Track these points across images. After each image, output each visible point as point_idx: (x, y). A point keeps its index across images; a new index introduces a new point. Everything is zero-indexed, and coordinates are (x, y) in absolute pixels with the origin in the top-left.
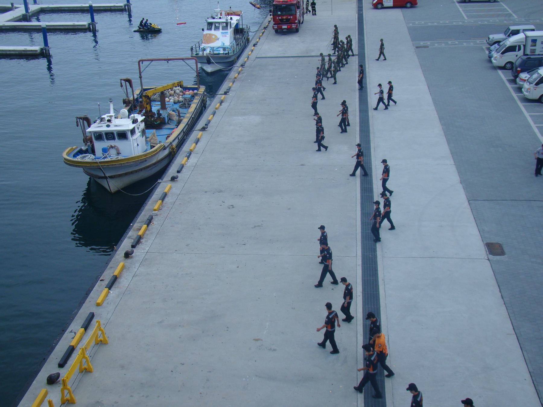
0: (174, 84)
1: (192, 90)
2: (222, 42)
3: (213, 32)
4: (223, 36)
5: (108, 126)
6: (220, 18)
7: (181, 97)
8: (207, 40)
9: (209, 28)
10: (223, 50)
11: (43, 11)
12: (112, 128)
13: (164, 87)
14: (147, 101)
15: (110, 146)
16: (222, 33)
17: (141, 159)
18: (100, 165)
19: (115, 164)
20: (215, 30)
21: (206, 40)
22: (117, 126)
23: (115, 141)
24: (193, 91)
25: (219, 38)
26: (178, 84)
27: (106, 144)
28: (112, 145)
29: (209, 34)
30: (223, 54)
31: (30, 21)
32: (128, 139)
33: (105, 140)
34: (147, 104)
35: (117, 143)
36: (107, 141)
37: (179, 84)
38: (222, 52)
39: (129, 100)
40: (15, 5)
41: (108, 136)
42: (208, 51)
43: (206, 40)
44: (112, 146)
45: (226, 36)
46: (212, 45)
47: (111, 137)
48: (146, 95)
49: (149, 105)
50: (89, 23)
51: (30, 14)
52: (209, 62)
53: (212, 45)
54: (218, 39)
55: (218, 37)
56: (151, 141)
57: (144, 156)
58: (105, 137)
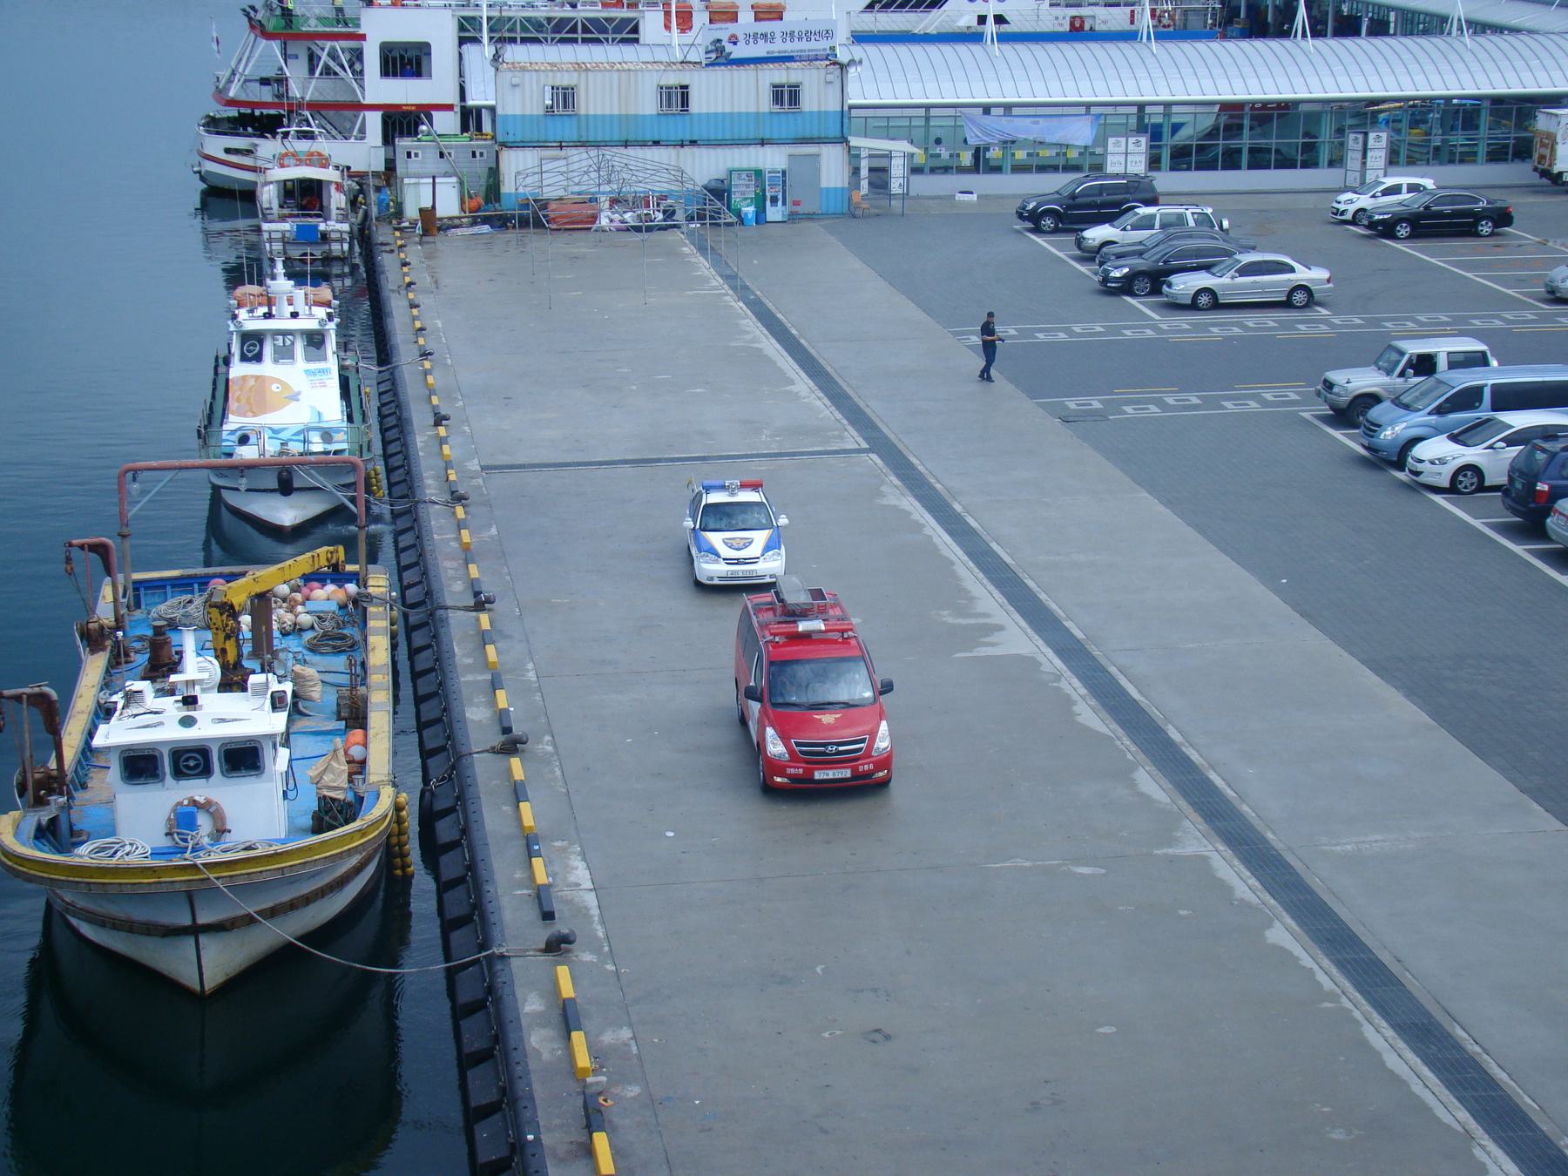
0: (316, 558)
1: (332, 583)
5: (187, 722)
7: (300, 608)
13: (283, 568)
14: (227, 625)
15: (186, 802)
17: (349, 850)
18: (211, 876)
19: (261, 872)
22: (223, 720)
24: (340, 587)
26: (329, 555)
27: (169, 795)
28: (197, 798)
32: (263, 772)
33: (169, 779)
35: (218, 789)
36: (175, 782)
37: (332, 558)
41: (181, 764)
44: (195, 801)
47: (196, 766)
48: (225, 600)
49: (233, 639)
56: (321, 777)
57: (360, 834)
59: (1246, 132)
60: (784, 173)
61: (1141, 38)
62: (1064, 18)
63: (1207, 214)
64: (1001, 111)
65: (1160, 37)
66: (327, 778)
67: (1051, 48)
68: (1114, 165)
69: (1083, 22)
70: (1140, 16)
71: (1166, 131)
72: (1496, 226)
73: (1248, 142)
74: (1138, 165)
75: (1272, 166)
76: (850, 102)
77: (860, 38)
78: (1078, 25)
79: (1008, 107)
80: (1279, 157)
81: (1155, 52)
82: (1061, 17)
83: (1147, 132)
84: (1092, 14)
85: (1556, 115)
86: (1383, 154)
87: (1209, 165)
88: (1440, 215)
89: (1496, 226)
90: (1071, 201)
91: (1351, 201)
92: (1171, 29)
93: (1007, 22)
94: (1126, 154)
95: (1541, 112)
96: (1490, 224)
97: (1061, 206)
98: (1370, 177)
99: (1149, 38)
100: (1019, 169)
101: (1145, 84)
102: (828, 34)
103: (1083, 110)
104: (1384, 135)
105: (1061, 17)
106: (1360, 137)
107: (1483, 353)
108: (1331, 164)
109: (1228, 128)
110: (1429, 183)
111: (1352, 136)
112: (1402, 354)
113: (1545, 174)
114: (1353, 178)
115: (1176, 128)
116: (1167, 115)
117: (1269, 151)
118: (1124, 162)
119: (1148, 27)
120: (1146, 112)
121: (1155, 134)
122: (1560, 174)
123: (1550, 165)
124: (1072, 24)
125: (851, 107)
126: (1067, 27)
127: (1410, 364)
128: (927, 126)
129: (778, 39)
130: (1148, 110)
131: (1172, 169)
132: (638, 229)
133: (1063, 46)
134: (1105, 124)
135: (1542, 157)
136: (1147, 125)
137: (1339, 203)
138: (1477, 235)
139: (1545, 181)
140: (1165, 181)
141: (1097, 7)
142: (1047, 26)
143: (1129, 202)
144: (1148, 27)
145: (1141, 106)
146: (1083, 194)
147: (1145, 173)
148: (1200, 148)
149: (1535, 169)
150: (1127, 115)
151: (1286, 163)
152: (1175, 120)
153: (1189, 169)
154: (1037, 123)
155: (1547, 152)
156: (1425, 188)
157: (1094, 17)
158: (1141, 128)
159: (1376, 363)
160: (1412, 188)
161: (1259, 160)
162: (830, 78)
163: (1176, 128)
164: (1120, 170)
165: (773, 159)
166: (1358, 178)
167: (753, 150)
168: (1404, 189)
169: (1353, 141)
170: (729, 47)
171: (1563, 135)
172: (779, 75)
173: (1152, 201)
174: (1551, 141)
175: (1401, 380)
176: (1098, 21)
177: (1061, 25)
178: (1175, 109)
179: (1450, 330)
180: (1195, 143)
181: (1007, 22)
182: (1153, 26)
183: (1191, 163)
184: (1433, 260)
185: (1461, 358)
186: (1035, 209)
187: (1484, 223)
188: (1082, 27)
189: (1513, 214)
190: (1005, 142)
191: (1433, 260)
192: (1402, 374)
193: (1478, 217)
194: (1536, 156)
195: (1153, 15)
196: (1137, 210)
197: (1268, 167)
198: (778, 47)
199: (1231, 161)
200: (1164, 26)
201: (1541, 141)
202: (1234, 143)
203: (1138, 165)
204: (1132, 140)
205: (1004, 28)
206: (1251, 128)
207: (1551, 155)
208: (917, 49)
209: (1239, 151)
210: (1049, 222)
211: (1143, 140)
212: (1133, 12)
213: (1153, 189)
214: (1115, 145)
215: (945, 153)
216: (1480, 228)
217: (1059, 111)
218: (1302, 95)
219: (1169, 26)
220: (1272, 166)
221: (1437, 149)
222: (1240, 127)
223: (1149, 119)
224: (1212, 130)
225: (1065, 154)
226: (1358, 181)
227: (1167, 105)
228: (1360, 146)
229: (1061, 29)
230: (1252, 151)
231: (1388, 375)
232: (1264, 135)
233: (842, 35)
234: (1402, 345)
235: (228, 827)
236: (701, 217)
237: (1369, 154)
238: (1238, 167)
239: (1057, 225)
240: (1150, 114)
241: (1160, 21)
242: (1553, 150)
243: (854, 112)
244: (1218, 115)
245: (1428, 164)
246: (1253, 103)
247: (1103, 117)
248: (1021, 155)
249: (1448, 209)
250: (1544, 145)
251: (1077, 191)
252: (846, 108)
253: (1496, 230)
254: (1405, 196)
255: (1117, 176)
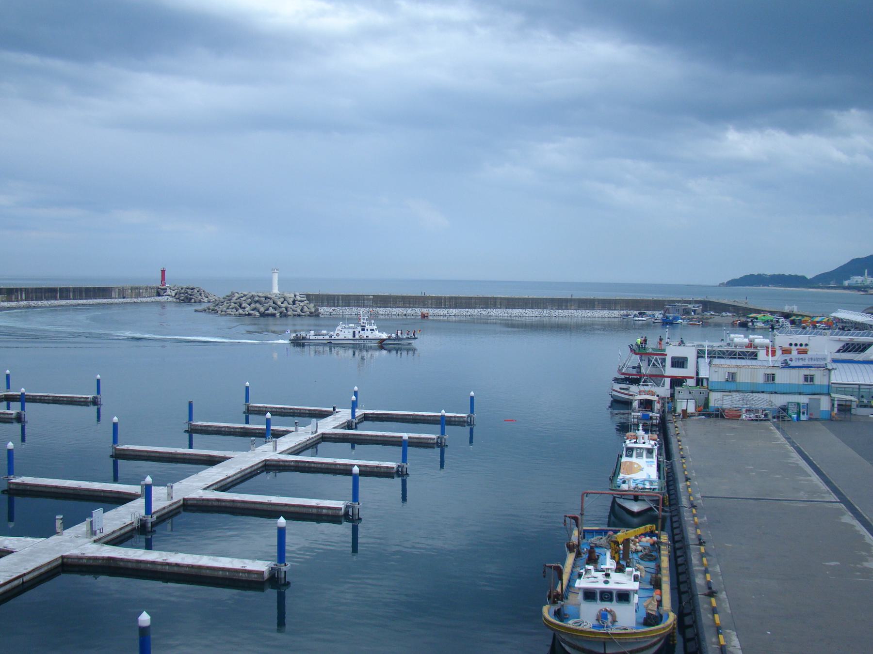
2: (647, 474)
3: (634, 459)
4: (648, 466)
5: (606, 582)
6: (644, 443)
8: (627, 470)
9: (628, 455)
10: (650, 483)
11: (366, 418)
12: (611, 586)
15: (603, 610)
16: (647, 462)
20: (637, 457)
21: (625, 469)
23: (613, 603)
25: (643, 468)
28: (607, 609)
29: (630, 462)
30: (650, 489)
31: (356, 428)
34: (616, 553)
35: (614, 606)
38: (648, 486)
39: (574, 544)
40: (337, 410)
41: (603, 596)
42: (633, 485)
43: (625, 469)
45: (651, 466)
46: (633, 476)
50: (438, 435)
51: (357, 421)
52: (636, 499)
53: (633, 476)
54: (642, 469)
55: (642, 467)
58: (598, 598)
60: (807, 404)
66: (650, 607)
76: (832, 382)
77: (835, 361)
102: (824, 359)
125: (833, 383)
128: (859, 391)
129: (807, 361)
132: (757, 420)
162: (825, 373)
165: (803, 399)
167: (797, 396)
170: (789, 362)
172: (807, 372)
198: (806, 363)
208: (856, 365)
215: (865, 401)
233: (829, 360)
235: (617, 620)
236: (778, 417)
243: (833, 385)
252: (830, 384)
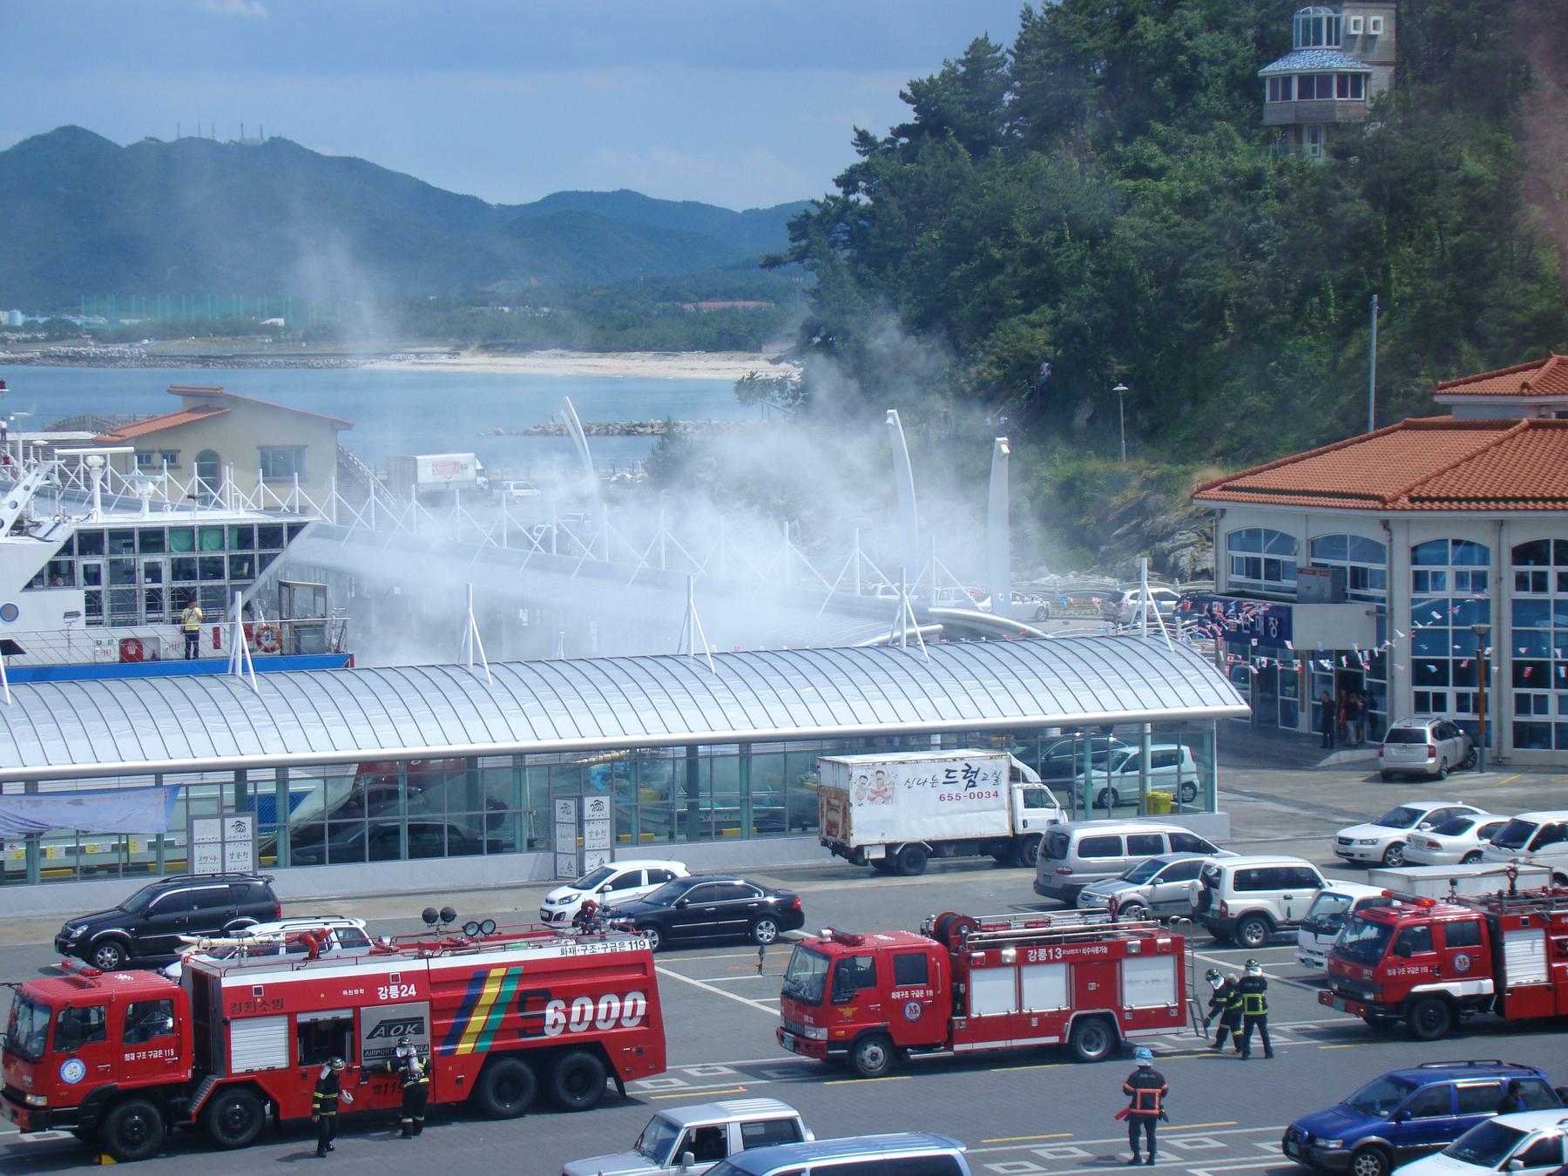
59: (402, 801)
61: (234, 670)
62: (110, 642)
63: (357, 929)
64: (20, 788)
65: (262, 666)
67: (92, 687)
68: (206, 862)
69: (140, 647)
70: (228, 636)
71: (281, 804)
72: (782, 927)
73: (407, 817)
74: (241, 860)
75: (446, 852)
78: (132, 652)
79: (31, 782)
80: (456, 837)
81: (256, 690)
82: (105, 641)
83: (253, 810)
84: (153, 634)
85: (846, 765)
86: (606, 827)
87: (350, 855)
88: (701, 915)
89: (782, 927)
90: (142, 920)
91: (568, 900)
92: (278, 652)
93: (20, 652)
94: (223, 843)
95: (824, 760)
96: (772, 926)
97: (127, 929)
98: (591, 865)
99: (245, 669)
100: (55, 875)
101: (246, 738)
103: (150, 781)
104: (606, 800)
105: (105, 641)
106: (572, 804)
107: (792, 1122)
108: (531, 845)
109: (375, 797)
110: (680, 870)
111: (559, 803)
112: (674, 1128)
113: (839, 849)
114: (566, 863)
115: (296, 799)
116: (282, 780)
117: (439, 829)
118: (219, 855)
119: (243, 651)
120: (248, 779)
121: (265, 810)
122: (860, 849)
123: (845, 836)
124: (123, 651)
126: (115, 656)
127: (687, 1145)
130: (251, 775)
131: (295, 863)
133: (113, 685)
134: (187, 799)
135: (832, 825)
136: (252, 798)
137: (552, 902)
138: (753, 941)
139: (840, 861)
140: (288, 881)
141: (162, 625)
142: (82, 655)
143: (233, 916)
144: (243, 651)
145: (240, 771)
146: (161, 908)
147: (254, 872)
148: (335, 829)
149: (825, 843)
150: (221, 784)
151: (465, 846)
152: (294, 788)
153: (320, 862)
154: (79, 803)
155: (838, 818)
156: (674, 876)
157: (157, 639)
158: (244, 803)
159: (637, 1146)
160: (655, 877)
161: (426, 843)
163: (296, 799)
164: (215, 868)
166: (574, 865)
168: (645, 878)
169: (564, 811)
171: (857, 793)
173: (271, 915)
174: (840, 802)
175: (674, 1169)
176: (163, 646)
177: (106, 653)
178: (293, 773)
179: (737, 1087)
180: (327, 822)
181: (20, 652)
182: (251, 651)
183: (324, 852)
184: (697, 983)
185: (761, 1131)
186: (86, 936)
187: (763, 924)
188: (139, 655)
189: (803, 909)
190: (30, 835)
191: (697, 983)
192: (678, 1160)
193: (762, 913)
194: (824, 824)
195: (248, 635)
196: (249, 929)
197: (439, 854)
199: (383, 846)
200: (266, 650)
201: (829, 803)
202: (385, 820)
203: (241, 860)
204: (230, 822)
205: (17, 660)
206: (410, 796)
207: (844, 822)
209: (395, 831)
210: (109, 955)
211: (248, 821)
212: (216, 630)
213: (267, 895)
214: (206, 830)
216: (759, 932)
217: (113, 783)
218: (482, 744)
219: (273, 649)
220: (446, 852)
221: (682, 817)
222: (393, 794)
223: (255, 789)
224: (350, 800)
225: (126, 848)
226: (574, 869)
227: (282, 768)
228: (572, 817)
229: (106, 659)
230: (414, 830)
231: (657, 1162)
232: (427, 805)
234: (674, 1114)
237: (587, 828)
238: (395, 856)
239: (121, 959)
240: (255, 782)
241: (259, 643)
242: (846, 815)
244: (357, 779)
245: (671, 837)
246: (407, 760)
247: (183, 789)
248: (55, 852)
249: (711, 905)
250: (832, 808)
251: (151, 906)
253: (781, 934)
254: (646, 889)
255: (213, 878)
